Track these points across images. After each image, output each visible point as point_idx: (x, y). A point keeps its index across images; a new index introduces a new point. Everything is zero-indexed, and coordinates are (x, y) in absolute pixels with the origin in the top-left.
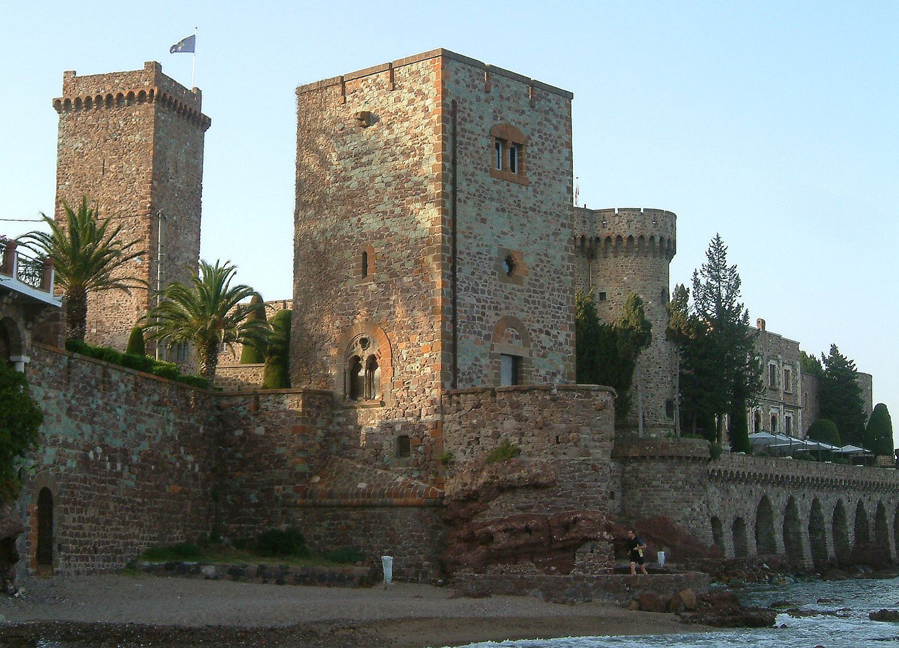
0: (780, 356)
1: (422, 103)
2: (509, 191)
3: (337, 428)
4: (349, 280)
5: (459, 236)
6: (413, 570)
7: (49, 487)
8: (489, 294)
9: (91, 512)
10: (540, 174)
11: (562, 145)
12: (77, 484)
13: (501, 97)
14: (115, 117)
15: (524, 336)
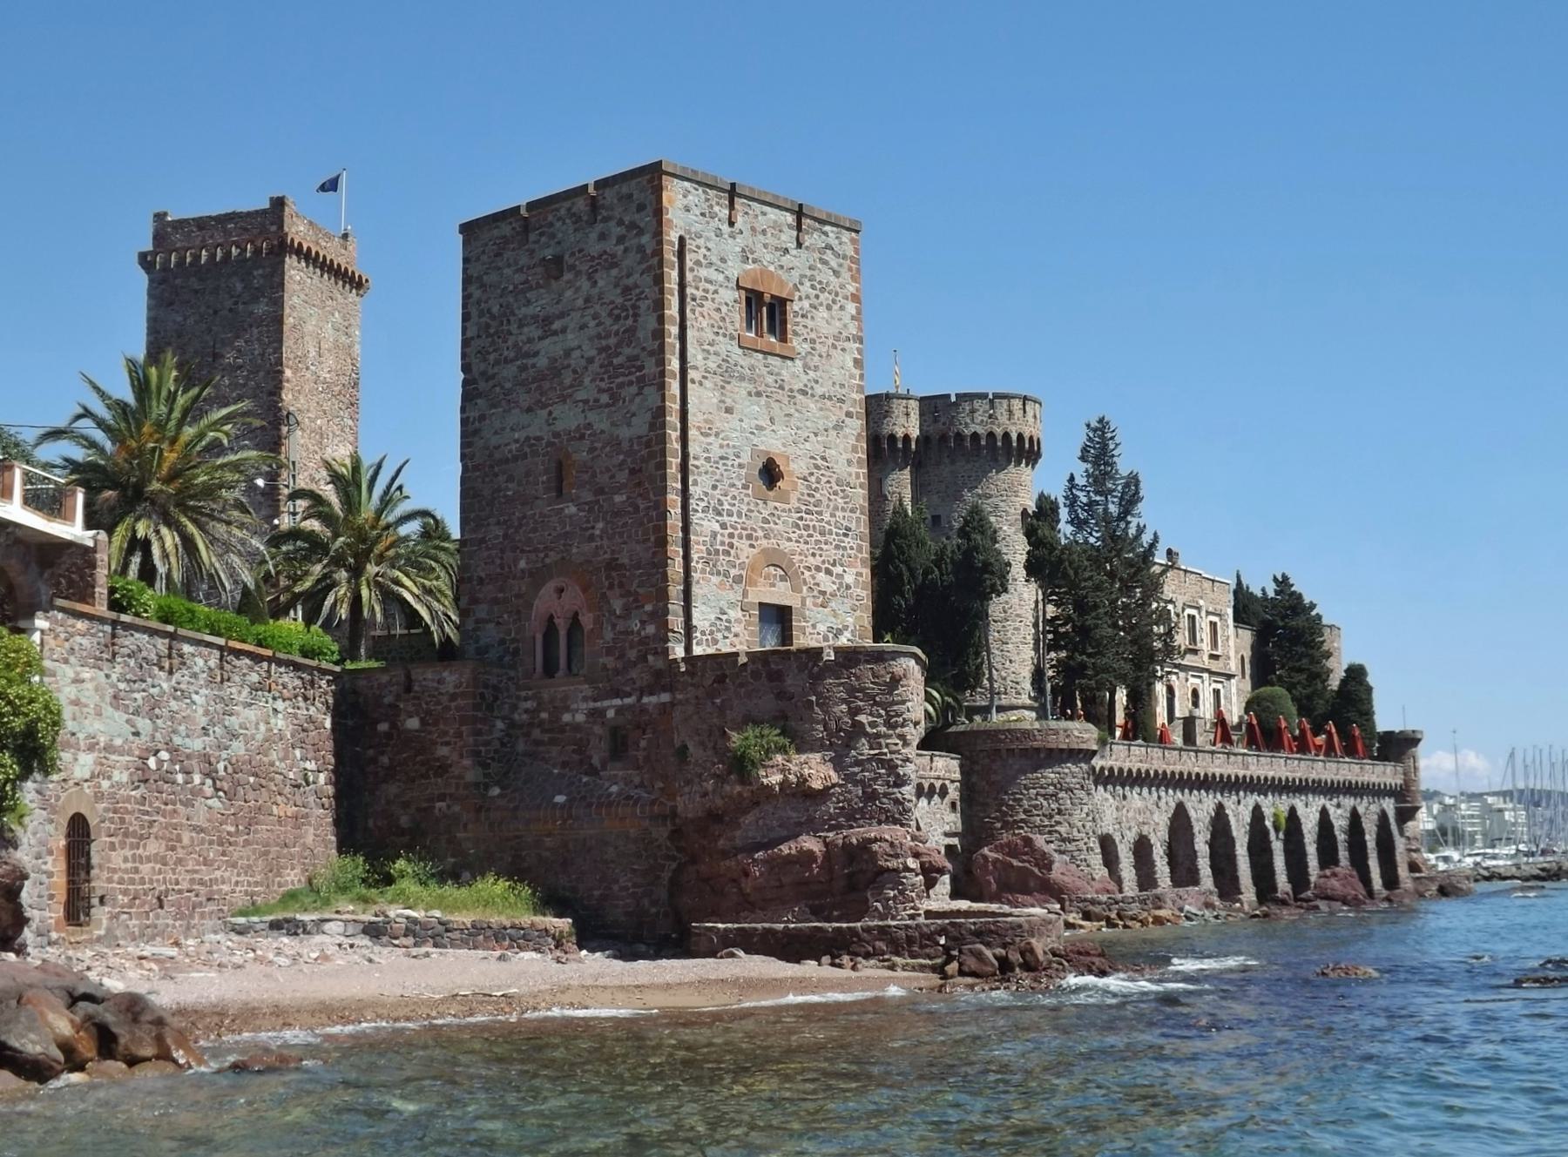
0: (1201, 602)
1: (635, 241)
3: (525, 716)
4: (539, 502)
5: (692, 433)
7: (83, 811)
8: (739, 514)
9: (153, 847)
10: (813, 341)
12: (129, 806)
13: (753, 229)
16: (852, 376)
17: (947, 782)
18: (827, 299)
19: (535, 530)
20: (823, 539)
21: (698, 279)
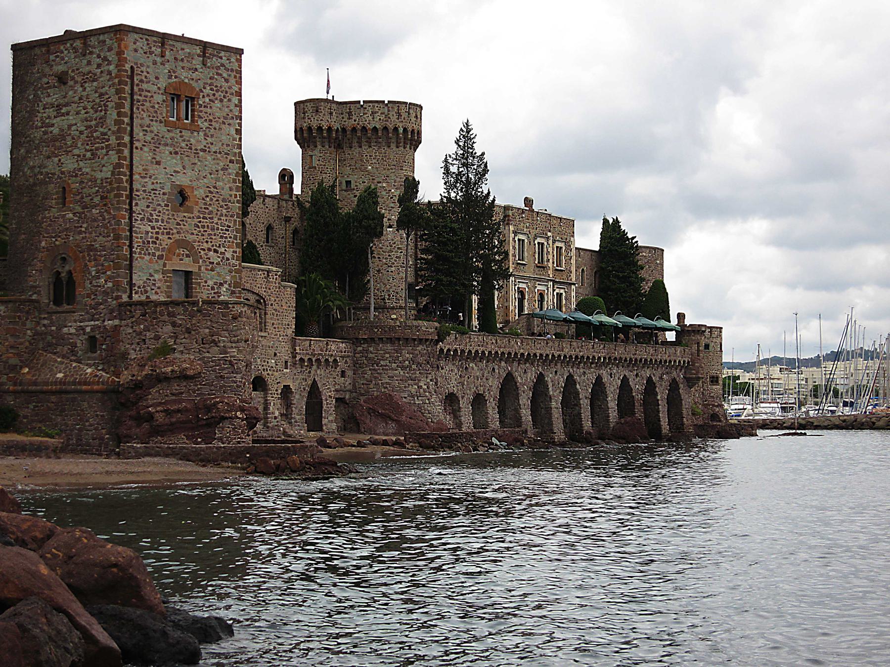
0: (549, 234)
1: (106, 68)
2: (181, 137)
3: (43, 328)
5: (136, 177)
6: (97, 442)
8: (163, 221)
10: (211, 121)
13: (176, 59)
15: (193, 253)
16: (234, 140)
17: (338, 358)
18: (220, 96)
19: (50, 225)
20: (213, 233)
21: (141, 90)
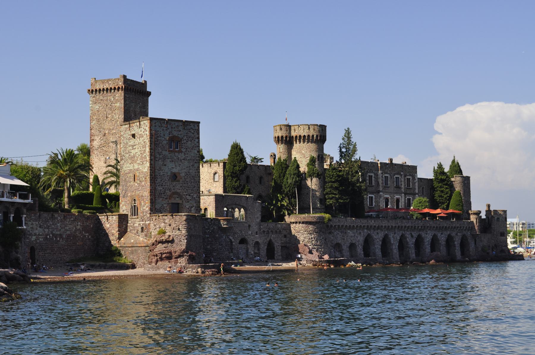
0: (402, 173)
1: (146, 133)
2: (175, 155)
8: (167, 186)
9: (48, 251)
10: (187, 149)
11: (196, 138)
13: (172, 128)
14: (110, 97)
